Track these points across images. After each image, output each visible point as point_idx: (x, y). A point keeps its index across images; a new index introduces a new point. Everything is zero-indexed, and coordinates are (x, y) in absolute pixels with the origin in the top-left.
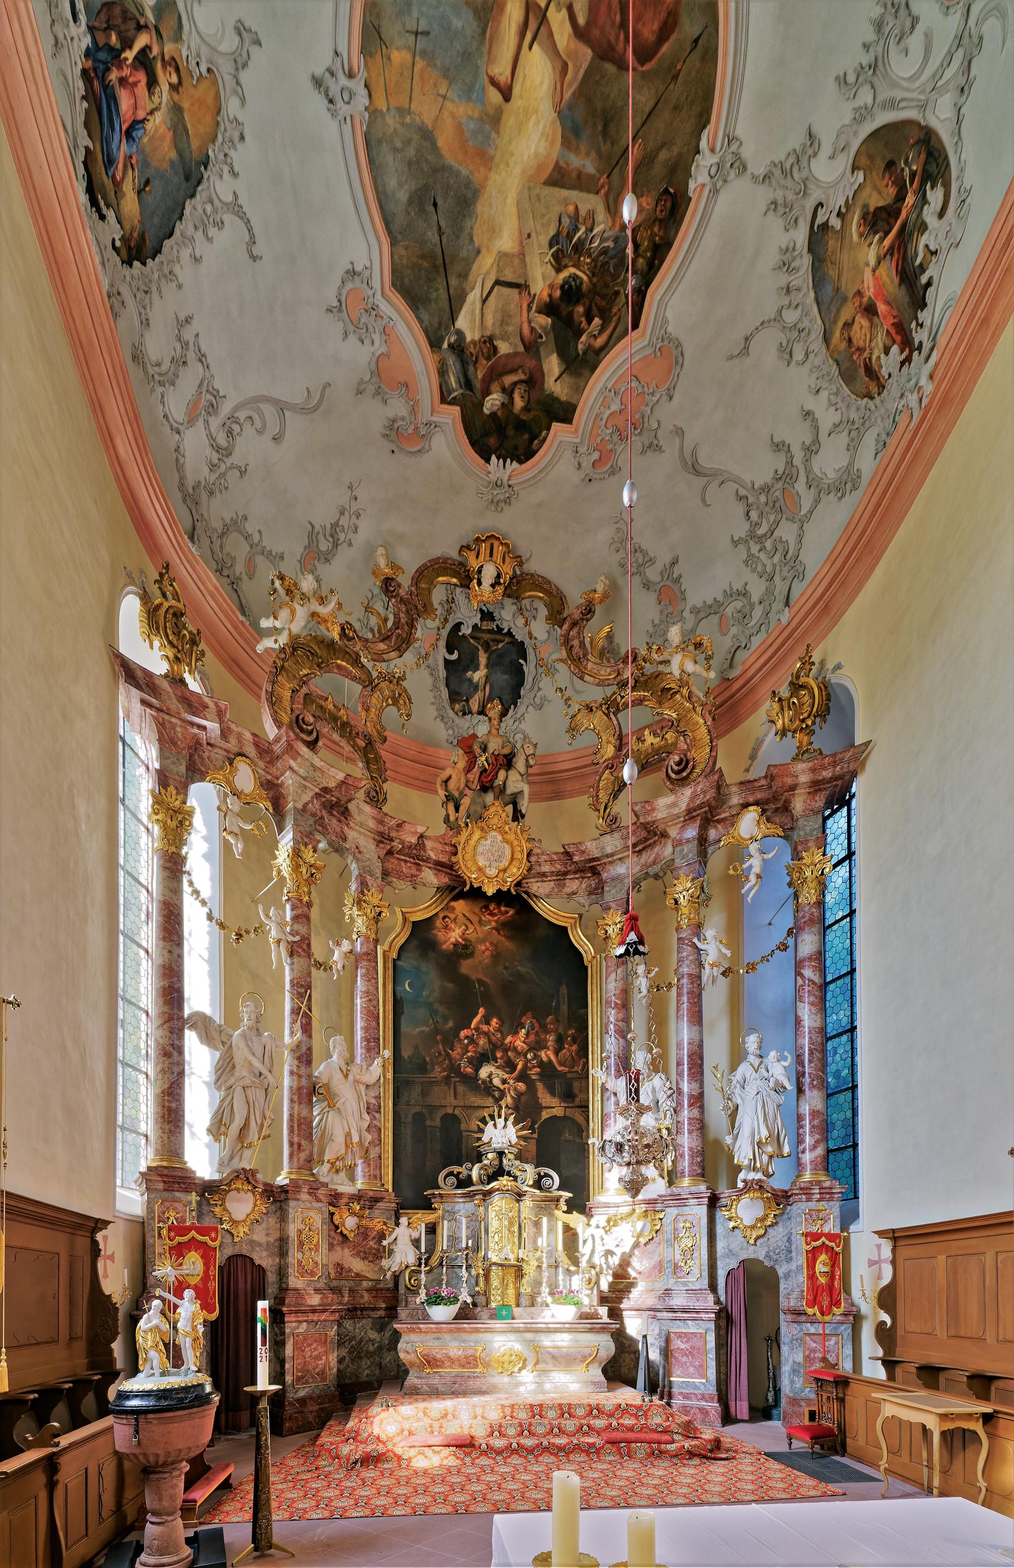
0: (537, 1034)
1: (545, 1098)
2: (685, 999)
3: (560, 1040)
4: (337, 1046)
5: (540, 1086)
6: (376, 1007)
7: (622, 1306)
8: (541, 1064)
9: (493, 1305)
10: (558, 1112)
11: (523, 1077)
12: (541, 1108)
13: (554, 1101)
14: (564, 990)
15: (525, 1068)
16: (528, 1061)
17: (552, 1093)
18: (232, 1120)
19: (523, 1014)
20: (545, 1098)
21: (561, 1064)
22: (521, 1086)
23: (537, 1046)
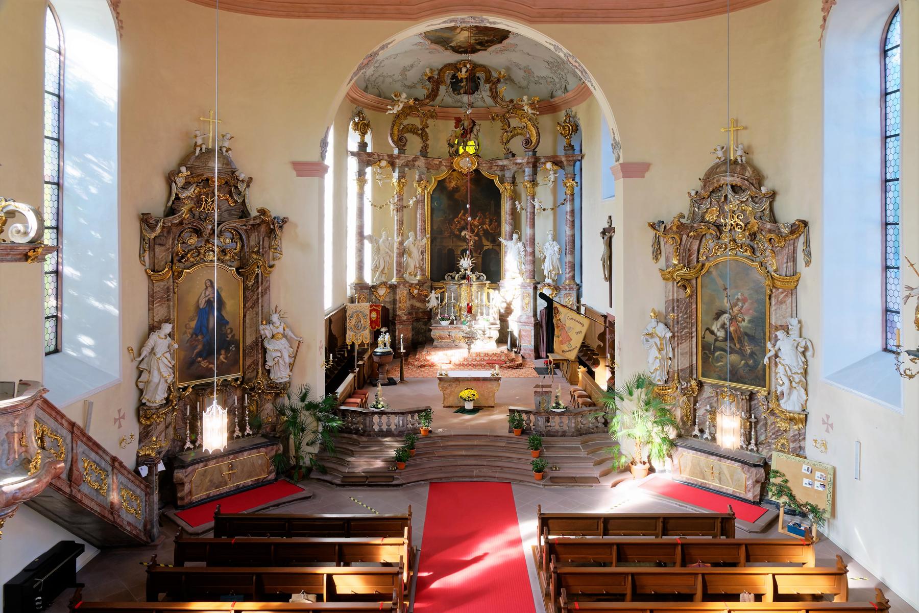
0: (482, 219)
1: (485, 242)
2: (528, 220)
3: (491, 221)
4: (411, 234)
5: (483, 238)
6: (425, 218)
7: (508, 319)
8: (484, 230)
9: (462, 320)
10: (490, 247)
11: (477, 235)
12: (483, 246)
13: (488, 243)
14: (492, 202)
15: (478, 232)
16: (479, 229)
17: (488, 241)
18: (380, 267)
19: (477, 212)
20: (485, 242)
21: (492, 230)
22: (476, 238)
23: (482, 224)
